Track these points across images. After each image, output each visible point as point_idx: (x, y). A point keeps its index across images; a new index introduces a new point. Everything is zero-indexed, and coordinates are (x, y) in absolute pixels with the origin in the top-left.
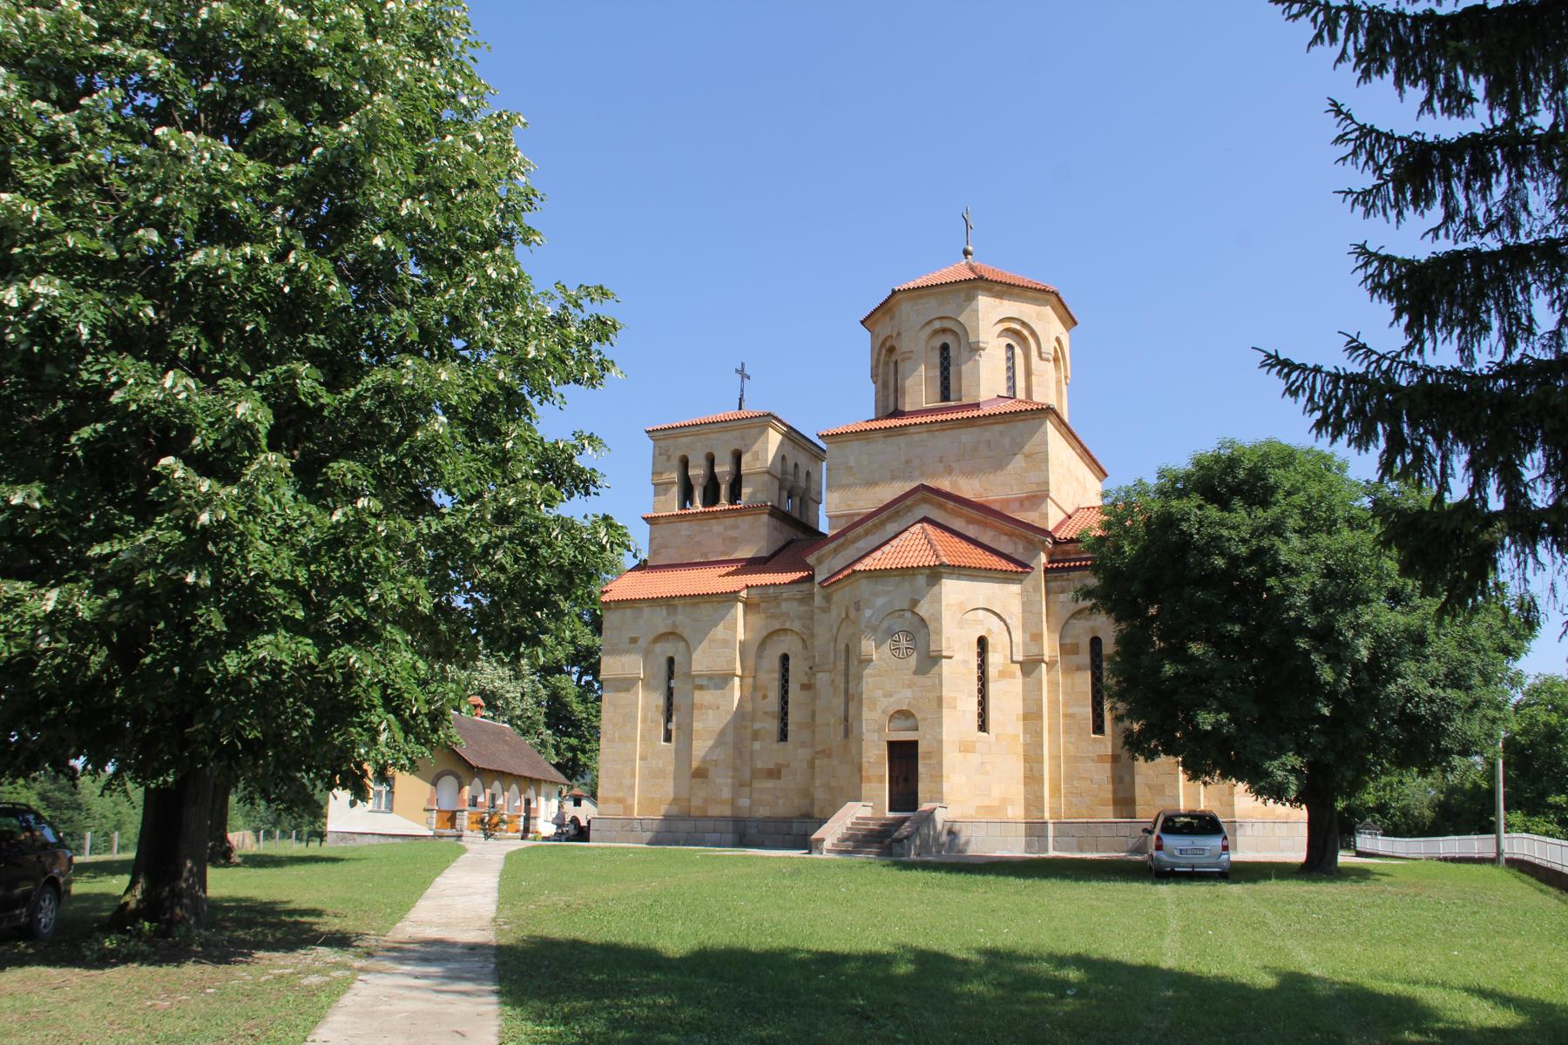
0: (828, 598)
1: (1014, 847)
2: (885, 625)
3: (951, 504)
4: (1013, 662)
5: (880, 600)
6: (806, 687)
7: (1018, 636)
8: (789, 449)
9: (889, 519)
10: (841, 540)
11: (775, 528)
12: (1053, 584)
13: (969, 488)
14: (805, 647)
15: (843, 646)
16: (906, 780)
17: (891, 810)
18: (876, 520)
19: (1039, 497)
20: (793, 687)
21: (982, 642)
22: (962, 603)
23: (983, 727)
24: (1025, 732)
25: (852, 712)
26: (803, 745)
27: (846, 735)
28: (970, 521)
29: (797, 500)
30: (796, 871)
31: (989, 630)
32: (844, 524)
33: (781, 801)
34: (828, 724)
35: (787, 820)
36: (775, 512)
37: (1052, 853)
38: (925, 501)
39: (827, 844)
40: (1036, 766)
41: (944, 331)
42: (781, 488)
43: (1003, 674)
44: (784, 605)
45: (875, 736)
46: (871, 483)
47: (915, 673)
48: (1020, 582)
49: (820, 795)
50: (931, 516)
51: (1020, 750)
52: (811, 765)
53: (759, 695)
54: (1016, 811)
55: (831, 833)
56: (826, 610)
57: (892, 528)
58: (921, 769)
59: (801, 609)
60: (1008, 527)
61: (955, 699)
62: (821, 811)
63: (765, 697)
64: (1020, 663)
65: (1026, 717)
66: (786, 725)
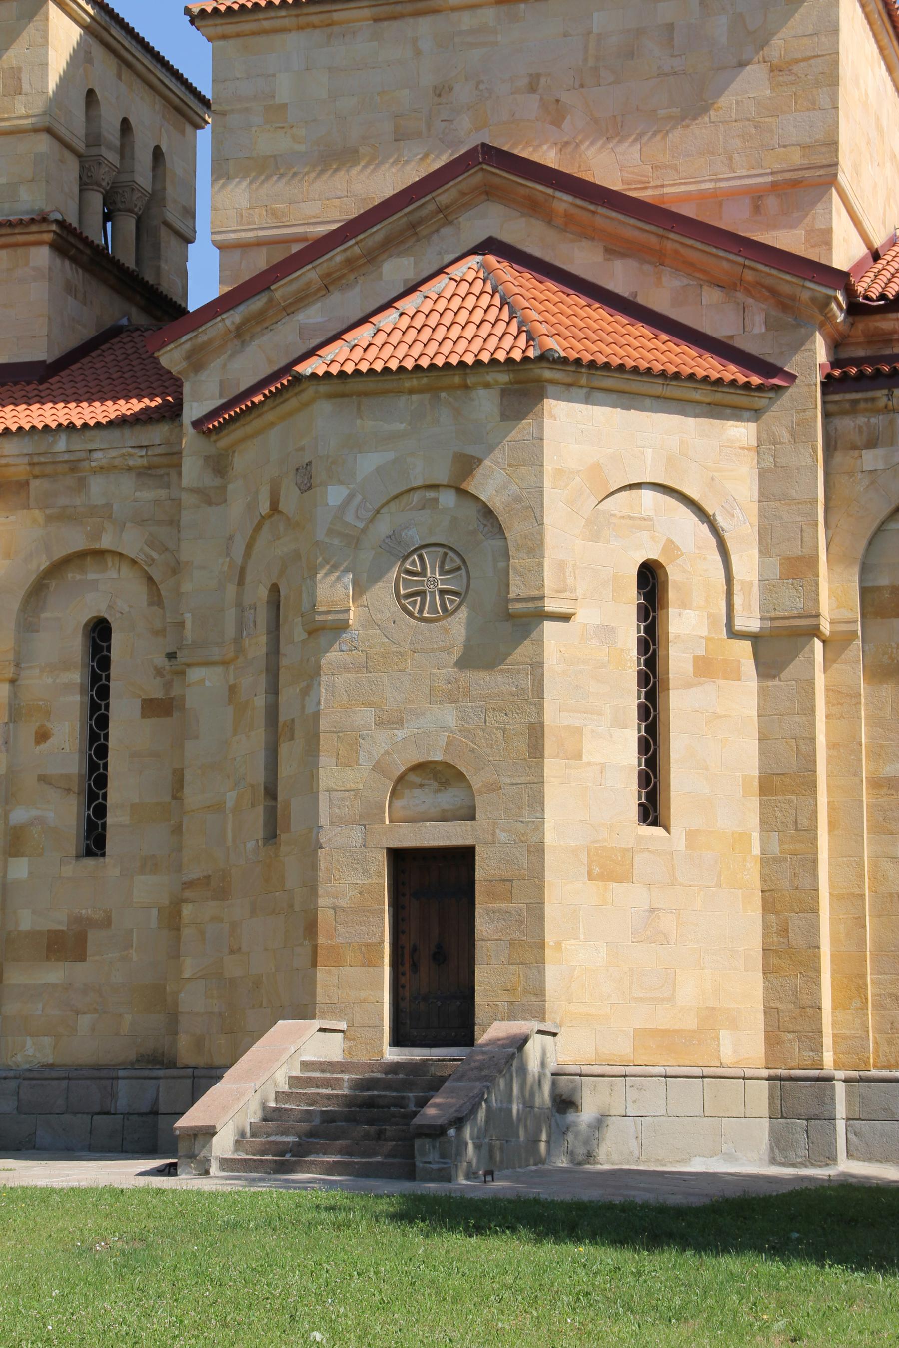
0: (219, 465)
1: (737, 1149)
2: (383, 527)
3: (563, 201)
4: (733, 633)
5: (369, 458)
6: (158, 708)
7: (747, 564)
8: (104, 74)
9: (389, 246)
10: (257, 304)
11: (70, 288)
12: (845, 424)
13: (608, 165)
14: (156, 597)
15: (263, 593)
16: (440, 956)
17: (398, 1041)
18: (353, 247)
19: (813, 180)
20: (123, 710)
21: (651, 580)
22: (596, 471)
23: (652, 810)
24: (766, 826)
25: (285, 771)
26: (149, 865)
27: (272, 835)
28: (617, 248)
29: (129, 224)
30: (134, 1249)
31: (670, 546)
32: (260, 262)
33: (85, 1021)
34: (218, 808)
35: (103, 1074)
36: (70, 243)
37: (848, 1166)
38: (490, 192)
39: (223, 1145)
40: (796, 921)
42: (85, 183)
43: (705, 668)
44: (97, 487)
45: (355, 836)
46: (336, 156)
47: (463, 663)
48: (756, 414)
49: (194, 1000)
50: (506, 237)
51: (752, 875)
52: (172, 918)
53: (27, 732)
54: (743, 1045)
55: (229, 1110)
56: (213, 498)
57: (396, 269)
59: (147, 495)
60: (725, 262)
61: (577, 731)
62: (199, 1044)
63: (43, 736)
64: (755, 638)
65: (768, 785)
66: (101, 811)
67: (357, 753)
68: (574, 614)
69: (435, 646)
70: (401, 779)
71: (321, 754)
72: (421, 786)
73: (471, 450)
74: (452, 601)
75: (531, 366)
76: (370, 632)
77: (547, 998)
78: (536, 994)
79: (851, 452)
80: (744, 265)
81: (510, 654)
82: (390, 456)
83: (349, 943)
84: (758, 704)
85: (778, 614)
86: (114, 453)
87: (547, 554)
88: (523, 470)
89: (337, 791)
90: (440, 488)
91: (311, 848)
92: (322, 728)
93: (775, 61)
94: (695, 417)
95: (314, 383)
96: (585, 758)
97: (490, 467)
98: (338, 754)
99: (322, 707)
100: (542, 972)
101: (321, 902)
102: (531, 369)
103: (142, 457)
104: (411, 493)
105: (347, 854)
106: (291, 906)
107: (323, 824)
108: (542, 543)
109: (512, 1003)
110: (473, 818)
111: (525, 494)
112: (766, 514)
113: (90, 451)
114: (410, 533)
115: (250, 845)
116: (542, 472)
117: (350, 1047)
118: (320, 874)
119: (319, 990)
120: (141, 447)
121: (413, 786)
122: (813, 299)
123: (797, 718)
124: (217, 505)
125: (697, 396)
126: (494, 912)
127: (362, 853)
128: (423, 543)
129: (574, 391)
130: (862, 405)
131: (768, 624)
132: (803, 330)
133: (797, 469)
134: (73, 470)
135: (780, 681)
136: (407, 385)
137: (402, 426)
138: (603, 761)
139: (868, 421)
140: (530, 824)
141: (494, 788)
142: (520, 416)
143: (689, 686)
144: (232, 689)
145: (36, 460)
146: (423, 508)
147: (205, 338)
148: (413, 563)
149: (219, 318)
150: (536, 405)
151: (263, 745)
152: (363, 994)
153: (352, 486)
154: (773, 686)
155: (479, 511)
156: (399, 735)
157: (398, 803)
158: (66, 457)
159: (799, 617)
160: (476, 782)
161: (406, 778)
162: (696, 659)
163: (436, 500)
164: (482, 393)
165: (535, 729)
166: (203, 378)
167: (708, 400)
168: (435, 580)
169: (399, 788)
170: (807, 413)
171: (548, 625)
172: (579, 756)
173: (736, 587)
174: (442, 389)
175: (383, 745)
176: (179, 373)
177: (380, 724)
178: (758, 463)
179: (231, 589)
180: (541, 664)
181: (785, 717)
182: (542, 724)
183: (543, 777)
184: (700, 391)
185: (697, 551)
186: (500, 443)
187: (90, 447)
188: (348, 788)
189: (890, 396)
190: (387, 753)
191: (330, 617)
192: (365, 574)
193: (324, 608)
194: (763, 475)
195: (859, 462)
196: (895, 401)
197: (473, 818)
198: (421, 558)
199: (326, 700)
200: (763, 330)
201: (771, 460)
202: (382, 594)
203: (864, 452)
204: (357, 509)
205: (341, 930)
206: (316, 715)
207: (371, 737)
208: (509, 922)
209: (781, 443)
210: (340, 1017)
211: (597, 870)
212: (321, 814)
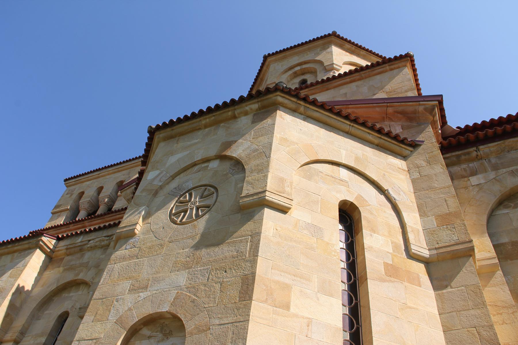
7: (413, 219)
12: (456, 169)
41: (304, 72)
48: (404, 158)
61: (287, 288)
68: (290, 208)
69: (185, 236)
75: (271, 96)
76: (146, 236)
79: (463, 179)
80: (387, 106)
82: (188, 152)
84: (438, 306)
85: (440, 245)
86: (97, 240)
87: (271, 170)
88: (261, 138)
89: (85, 340)
94: (370, 147)
96: (293, 309)
102: (271, 98)
103: (107, 240)
108: (268, 165)
113: (89, 241)
120: (108, 236)
122: (425, 109)
123: (472, 312)
125: (370, 138)
129: (296, 114)
130: (463, 157)
131: (435, 252)
132: (423, 126)
133: (435, 175)
134: (81, 250)
135: (452, 288)
136: (204, 122)
138: (310, 317)
139: (468, 166)
141: (204, 329)
143: (383, 280)
145: (69, 247)
146: (199, 171)
154: (447, 292)
158: (80, 244)
159: (457, 244)
162: (386, 265)
163: (208, 166)
165: (247, 279)
167: (376, 141)
170: (434, 153)
171: (267, 212)
172: (287, 307)
173: (409, 230)
175: (129, 304)
177: (133, 290)
178: (410, 177)
180: (259, 234)
181: (463, 312)
182: (254, 274)
183: (249, 315)
185: (379, 206)
187: (89, 239)
188: (93, 337)
189: (478, 150)
190: (130, 309)
191: (125, 230)
194: (414, 181)
195: (469, 182)
196: (481, 152)
200: (401, 130)
203: (470, 178)
207: (123, 299)
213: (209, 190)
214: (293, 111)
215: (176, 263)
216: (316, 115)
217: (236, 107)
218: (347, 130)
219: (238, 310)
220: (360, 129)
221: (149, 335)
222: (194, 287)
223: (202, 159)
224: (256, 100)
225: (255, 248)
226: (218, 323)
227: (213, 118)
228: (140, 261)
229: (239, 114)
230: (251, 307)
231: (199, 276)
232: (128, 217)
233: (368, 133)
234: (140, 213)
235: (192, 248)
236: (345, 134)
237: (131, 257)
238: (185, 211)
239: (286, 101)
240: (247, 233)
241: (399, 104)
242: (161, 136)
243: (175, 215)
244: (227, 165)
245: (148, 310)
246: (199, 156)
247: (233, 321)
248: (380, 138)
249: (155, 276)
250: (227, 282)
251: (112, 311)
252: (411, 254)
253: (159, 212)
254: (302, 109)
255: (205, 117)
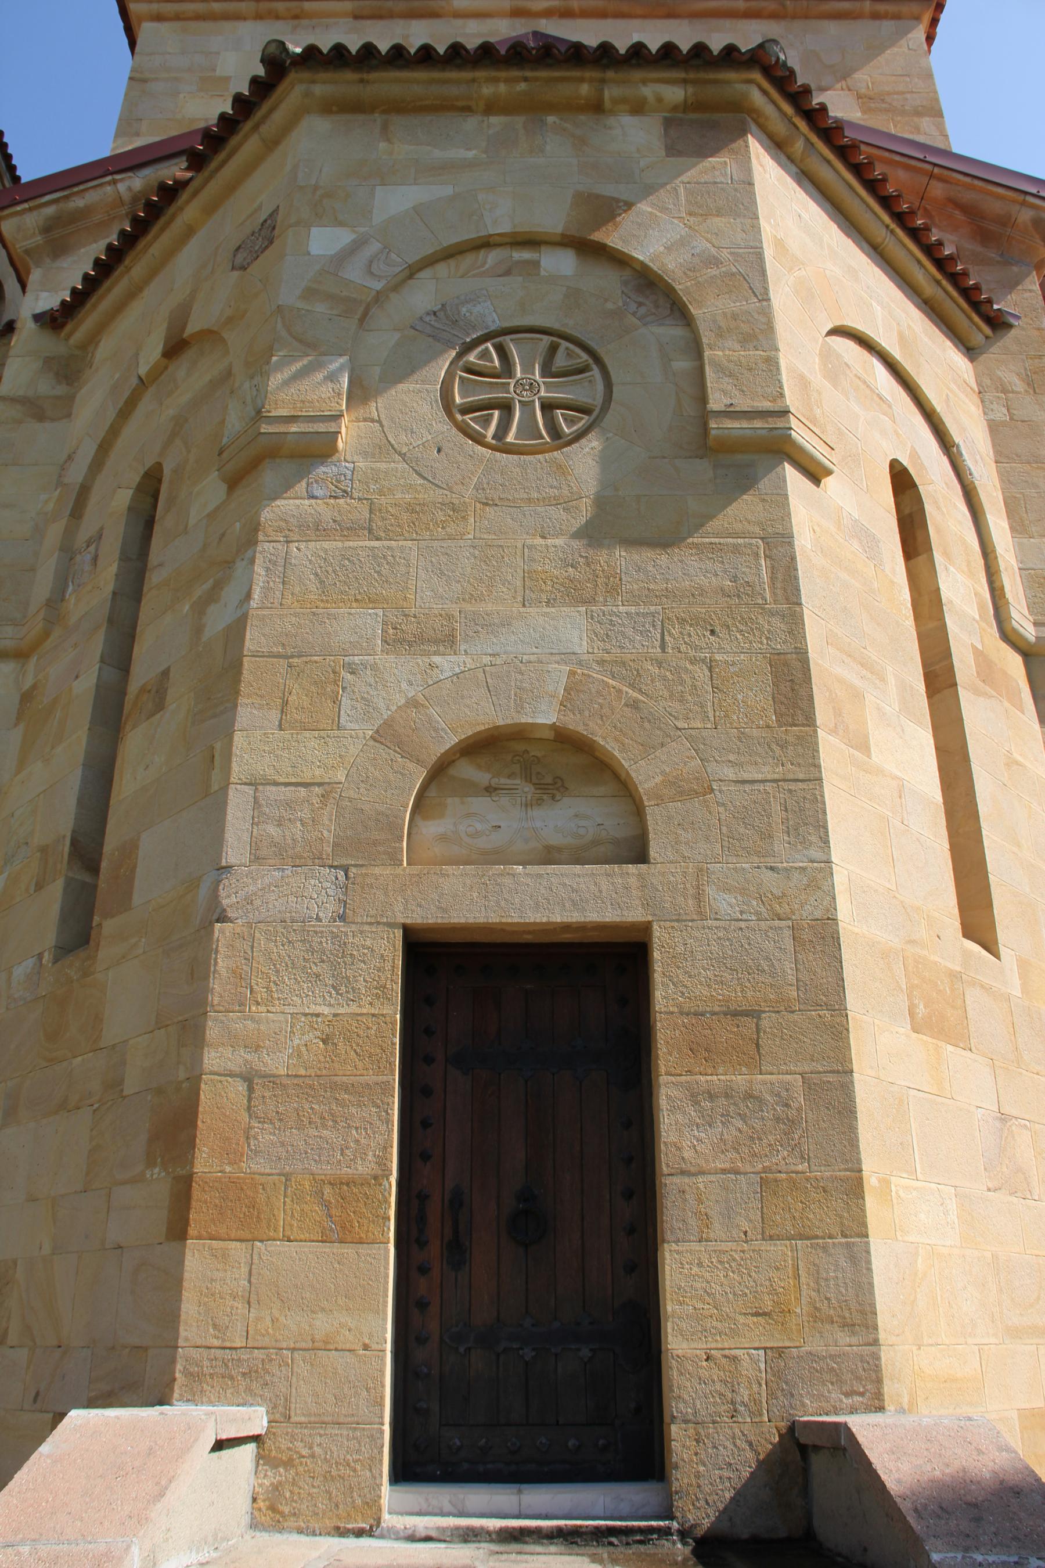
2: (422, 296)
15: (124, 498)
25: (127, 784)
27: (78, 934)
45: (317, 893)
48: (970, 351)
58: (681, 1131)
61: (857, 696)
67: (336, 700)
68: (829, 473)
70: (439, 772)
71: (241, 700)
72: (490, 790)
73: (608, 190)
74: (570, 421)
75: (731, 75)
76: (383, 466)
77: (882, 1336)
78: (849, 1326)
80: (931, 176)
81: (711, 517)
82: (448, 190)
83: (288, 1177)
88: (718, 222)
89: (276, 784)
90: (543, 248)
91: (195, 922)
92: (249, 645)
93: (863, 91)
95: (306, 75)
97: (651, 213)
98: (285, 703)
99: (253, 604)
100: (859, 1260)
101: (212, 1059)
102: (728, 82)
104: (482, 252)
105: (293, 937)
106: (114, 1084)
107: (232, 860)
109: (780, 1352)
110: (641, 857)
111: (725, 254)
112: (1011, 479)
114: (478, 309)
115: (20, 972)
116: (756, 229)
117: (276, 1488)
118: (216, 985)
119: (189, 1308)
121: (469, 789)
122: (1036, 222)
124: (53, 420)
125: (920, 277)
126: (711, 1097)
127: (335, 936)
128: (507, 324)
132: (1015, 269)
136: (487, 90)
137: (470, 154)
138: (899, 774)
140: (796, 875)
142: (704, 152)
144: (27, 697)
146: (508, 273)
147: (79, 203)
148: (485, 355)
149: (109, 178)
150: (733, 141)
151: (81, 758)
152: (322, 1325)
153: (362, 230)
155: (625, 283)
156: (446, 666)
157: (431, 829)
160: (645, 775)
161: (452, 771)
163: (536, 264)
164: (627, 120)
165: (786, 664)
166: (65, 265)
167: (929, 290)
168: (532, 386)
169: (432, 792)
172: (864, 747)
174: (551, 107)
175: (404, 685)
176: (27, 252)
177: (397, 641)
178: (985, 413)
179: (55, 532)
180: (787, 538)
184: (923, 270)
186: (667, 184)
188: (307, 777)
190: (413, 703)
191: (294, 428)
192: (377, 370)
193: (284, 412)
194: (994, 428)
197: (641, 857)
198: (501, 350)
199: (267, 590)
201: (1006, 412)
202: (415, 405)
204: (371, 262)
205: (265, 1137)
206: (237, 630)
207: (374, 667)
208: (758, 1125)
209: (1013, 392)
210: (249, 1390)
211: (921, 1010)
212: (230, 836)
213: (572, 353)
214: (778, 146)
215: (529, 576)
216: (825, 173)
217: (610, 74)
218: (879, 240)
219: (782, 747)
220: (904, 246)
221: (487, 784)
222: (624, 663)
223: (514, 234)
224: (682, 75)
225: (784, 580)
226: (732, 776)
227: (523, 86)
228: (389, 548)
229: (615, 101)
230: (817, 744)
231: (629, 632)
232: (287, 383)
233: (919, 262)
234: (332, 377)
235: (576, 535)
236: (871, 251)
237: (348, 530)
238: (506, 408)
239: (769, 110)
240: (751, 528)
241: (968, 180)
242: (318, 89)
243: (466, 410)
244: (605, 281)
245: (485, 714)
246: (501, 219)
247: (776, 776)
248: (938, 282)
249: (468, 607)
250: (726, 662)
251: (346, 702)
252: (1008, 629)
253: (400, 386)
254: (799, 145)
255: (494, 74)
